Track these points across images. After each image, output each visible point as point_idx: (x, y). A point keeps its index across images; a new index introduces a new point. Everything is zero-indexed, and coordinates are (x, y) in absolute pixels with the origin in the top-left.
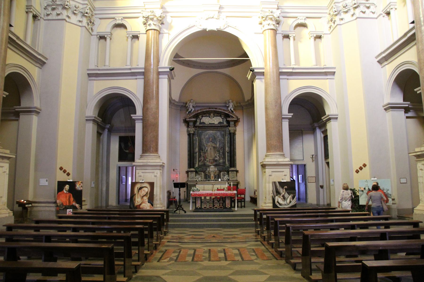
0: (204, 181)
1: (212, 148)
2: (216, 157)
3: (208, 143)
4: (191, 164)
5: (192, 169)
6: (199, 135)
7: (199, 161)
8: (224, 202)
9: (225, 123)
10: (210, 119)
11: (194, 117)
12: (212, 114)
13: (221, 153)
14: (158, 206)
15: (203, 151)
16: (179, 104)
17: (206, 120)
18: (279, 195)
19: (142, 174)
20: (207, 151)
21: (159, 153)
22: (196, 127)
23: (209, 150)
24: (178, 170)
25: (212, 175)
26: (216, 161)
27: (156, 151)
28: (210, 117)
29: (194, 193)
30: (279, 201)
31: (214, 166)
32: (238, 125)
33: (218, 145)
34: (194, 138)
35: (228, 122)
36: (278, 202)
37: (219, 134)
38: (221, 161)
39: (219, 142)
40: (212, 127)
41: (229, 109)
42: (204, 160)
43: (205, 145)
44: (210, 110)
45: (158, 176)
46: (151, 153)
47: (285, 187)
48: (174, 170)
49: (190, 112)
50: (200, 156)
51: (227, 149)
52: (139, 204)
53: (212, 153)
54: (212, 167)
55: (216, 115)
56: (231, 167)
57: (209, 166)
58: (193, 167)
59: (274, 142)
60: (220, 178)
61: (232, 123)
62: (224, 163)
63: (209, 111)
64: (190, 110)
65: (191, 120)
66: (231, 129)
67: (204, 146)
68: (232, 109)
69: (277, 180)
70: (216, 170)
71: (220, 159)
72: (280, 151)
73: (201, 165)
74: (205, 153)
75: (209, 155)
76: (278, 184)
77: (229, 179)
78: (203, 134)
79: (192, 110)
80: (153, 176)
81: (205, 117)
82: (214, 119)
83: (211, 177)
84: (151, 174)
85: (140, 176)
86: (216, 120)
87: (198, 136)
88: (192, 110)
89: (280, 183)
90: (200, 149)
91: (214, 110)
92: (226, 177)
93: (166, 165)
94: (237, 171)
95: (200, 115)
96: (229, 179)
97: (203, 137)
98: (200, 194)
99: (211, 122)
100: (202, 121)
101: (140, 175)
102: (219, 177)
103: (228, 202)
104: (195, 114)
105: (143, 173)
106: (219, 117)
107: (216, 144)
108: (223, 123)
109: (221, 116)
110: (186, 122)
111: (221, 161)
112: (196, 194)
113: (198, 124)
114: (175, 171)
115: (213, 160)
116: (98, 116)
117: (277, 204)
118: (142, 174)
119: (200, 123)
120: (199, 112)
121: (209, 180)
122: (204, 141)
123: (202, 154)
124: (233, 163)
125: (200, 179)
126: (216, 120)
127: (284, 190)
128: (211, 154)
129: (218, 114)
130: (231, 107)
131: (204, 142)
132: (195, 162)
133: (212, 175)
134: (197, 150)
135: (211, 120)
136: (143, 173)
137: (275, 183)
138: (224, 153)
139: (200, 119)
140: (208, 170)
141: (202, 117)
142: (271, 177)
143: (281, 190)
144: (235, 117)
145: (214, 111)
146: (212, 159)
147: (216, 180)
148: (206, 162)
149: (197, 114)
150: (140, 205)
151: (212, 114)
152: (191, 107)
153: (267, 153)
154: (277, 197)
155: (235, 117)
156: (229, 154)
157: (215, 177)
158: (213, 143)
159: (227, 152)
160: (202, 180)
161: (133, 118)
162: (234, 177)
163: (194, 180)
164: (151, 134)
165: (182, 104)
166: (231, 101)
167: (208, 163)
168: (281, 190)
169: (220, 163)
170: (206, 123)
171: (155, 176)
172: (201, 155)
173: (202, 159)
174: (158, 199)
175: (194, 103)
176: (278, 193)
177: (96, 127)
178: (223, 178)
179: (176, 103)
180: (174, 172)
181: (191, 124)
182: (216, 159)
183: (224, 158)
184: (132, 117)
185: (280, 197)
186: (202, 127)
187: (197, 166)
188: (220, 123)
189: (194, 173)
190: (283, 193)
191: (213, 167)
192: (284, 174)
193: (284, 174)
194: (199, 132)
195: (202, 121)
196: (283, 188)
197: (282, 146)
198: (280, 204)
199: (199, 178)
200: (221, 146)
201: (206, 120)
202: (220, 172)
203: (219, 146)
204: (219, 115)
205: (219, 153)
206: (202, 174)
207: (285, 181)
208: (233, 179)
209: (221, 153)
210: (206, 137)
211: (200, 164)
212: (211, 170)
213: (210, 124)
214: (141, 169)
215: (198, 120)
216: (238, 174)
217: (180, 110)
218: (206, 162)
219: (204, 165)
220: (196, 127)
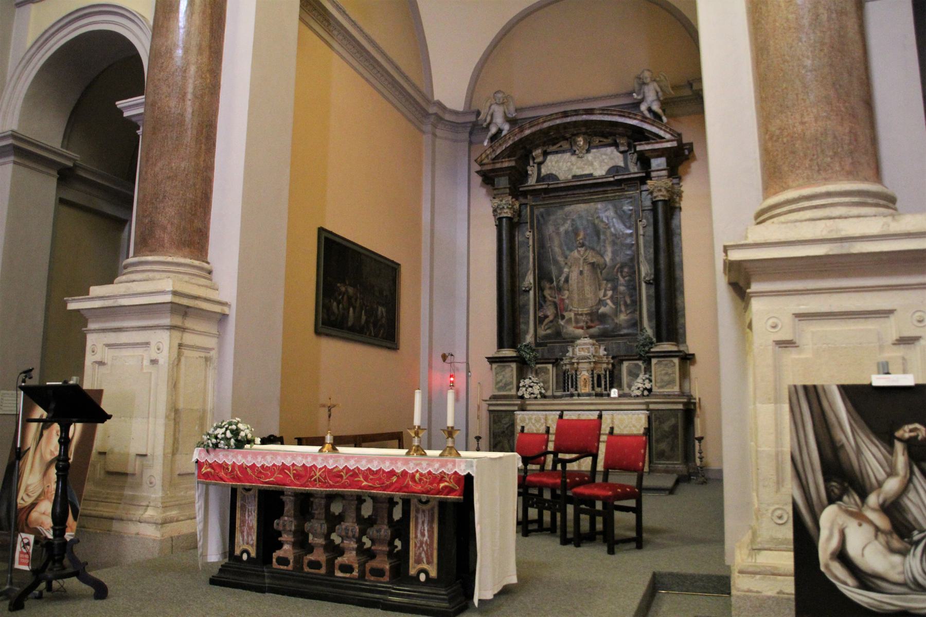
0: (554, 397)
1: (586, 269)
2: (601, 302)
3: (571, 250)
4: (508, 331)
5: (508, 353)
6: (539, 228)
7: (539, 321)
8: (401, 530)
9: (634, 170)
10: (574, 158)
11: (510, 152)
12: (581, 141)
13: (622, 288)
14: (150, 512)
15: (551, 281)
16: (461, 120)
17: (562, 166)
18: (850, 500)
19: (107, 355)
20: (567, 281)
21: (209, 259)
22: (525, 194)
23: (574, 276)
24: (460, 356)
25: (584, 375)
26: (602, 318)
27: (195, 240)
28: (574, 153)
29: (211, 458)
30: (853, 550)
31: (592, 337)
32: (686, 173)
33: (608, 258)
34: (519, 238)
35: (644, 160)
36: (842, 556)
37: (611, 213)
38: (623, 317)
39: (614, 243)
40: (586, 188)
41: (643, 107)
42: (556, 316)
43: (561, 259)
44: (568, 120)
45: (161, 362)
46: (153, 252)
47: (905, 432)
48: (444, 357)
49: (494, 138)
50: (541, 302)
51: (645, 270)
52: (29, 501)
53: (587, 288)
54: (582, 341)
55: (596, 140)
56: (660, 339)
57: (572, 340)
58: (513, 346)
59: (810, 116)
60: (620, 387)
61: (658, 163)
62: (636, 324)
63: (566, 126)
64: (493, 130)
65: (498, 166)
66: (659, 183)
67: (556, 262)
68: (656, 107)
69: (831, 377)
70: (602, 352)
71: (617, 312)
72: (852, 174)
73: (547, 337)
74: (559, 290)
75: (576, 296)
76: (840, 408)
77: (650, 390)
78: (552, 218)
79: (500, 131)
80: (146, 362)
81: (557, 152)
82: (590, 157)
83: (581, 383)
84: (139, 351)
85: (101, 363)
86: (600, 162)
87: (532, 227)
88: (500, 131)
89: (860, 397)
90: (543, 276)
91: (585, 117)
92: (640, 383)
93: (232, 312)
94: (687, 359)
95: (537, 147)
96: (650, 390)
97: (550, 229)
98: (242, 468)
99: (579, 172)
100: (544, 171)
101: (97, 358)
102: (614, 380)
103: (424, 537)
104: (515, 145)
105: (109, 346)
106: (609, 150)
107: (602, 256)
108: (626, 168)
109: (615, 145)
110: (488, 178)
111: (623, 317)
112: (223, 466)
113: (532, 181)
114: (449, 359)
115: (590, 314)
116: (62, 147)
117: (837, 573)
118: (107, 355)
119: (540, 179)
120: (527, 132)
121: (572, 395)
122: (556, 247)
123: (547, 293)
124: (669, 322)
125: (536, 390)
126: (600, 162)
127: (901, 459)
128: (581, 291)
129: (602, 133)
130: (651, 100)
131: (557, 250)
132: (523, 326)
133: (584, 375)
134: (530, 279)
135: (580, 163)
136: (109, 346)
137: (813, 394)
138: (633, 288)
139: (540, 164)
140: (570, 354)
141: (545, 154)
142: (791, 356)
143: (869, 456)
144: (668, 136)
145: (586, 123)
146: (586, 310)
147: (597, 395)
148: (562, 323)
149: (520, 140)
150: (33, 505)
151: (581, 141)
152: (499, 120)
153: (765, 198)
154: (830, 516)
155: (668, 136)
156: (652, 291)
157: (597, 381)
158: (593, 249)
159: (648, 283)
160: (549, 393)
161: (126, 114)
162: (671, 383)
163: (513, 392)
164: (160, 165)
165: (473, 118)
166: (647, 74)
167: (571, 329)
168: (869, 456)
169: (618, 327)
170: (562, 176)
171: (154, 362)
172: (544, 297)
173: (550, 312)
174: (158, 481)
175: (512, 108)
176: (842, 478)
177: (46, 187)
178: (630, 386)
179: (447, 117)
180: (446, 366)
181: (503, 182)
182: (602, 310)
183: (635, 304)
184: (120, 112)
185: (859, 517)
186: (546, 191)
187: (529, 338)
188: (614, 170)
189: (514, 365)
190: (892, 485)
191: (588, 340)
192: (892, 329)
193: (892, 329)
194: (536, 212)
195: (544, 171)
196: (887, 438)
197: (874, 140)
198: (865, 579)
199: (533, 386)
200: (621, 259)
201: (562, 166)
202: (618, 360)
203: (612, 260)
204: (609, 141)
205: (614, 289)
206: (546, 371)
207: (907, 380)
208: (666, 390)
209: (622, 288)
210: (562, 229)
211: (542, 332)
212: (579, 353)
213: (574, 177)
214: (104, 330)
215: (532, 170)
216: (694, 370)
217: (471, 143)
218: (562, 323)
219: (558, 334)
220: (525, 194)
